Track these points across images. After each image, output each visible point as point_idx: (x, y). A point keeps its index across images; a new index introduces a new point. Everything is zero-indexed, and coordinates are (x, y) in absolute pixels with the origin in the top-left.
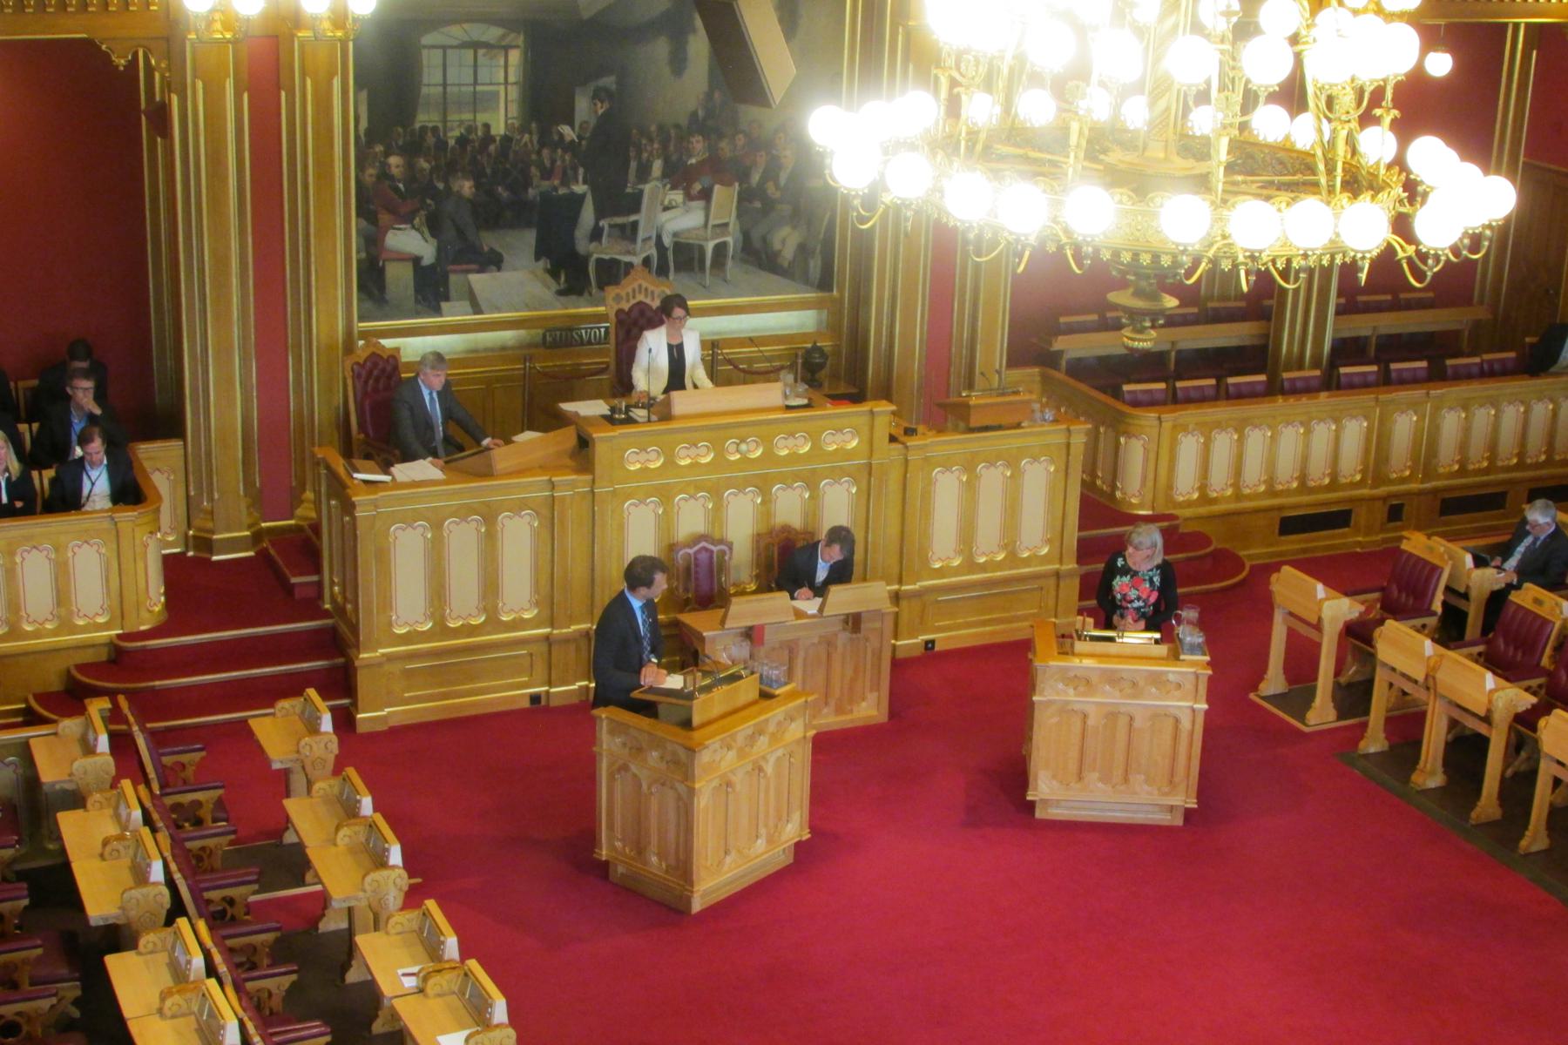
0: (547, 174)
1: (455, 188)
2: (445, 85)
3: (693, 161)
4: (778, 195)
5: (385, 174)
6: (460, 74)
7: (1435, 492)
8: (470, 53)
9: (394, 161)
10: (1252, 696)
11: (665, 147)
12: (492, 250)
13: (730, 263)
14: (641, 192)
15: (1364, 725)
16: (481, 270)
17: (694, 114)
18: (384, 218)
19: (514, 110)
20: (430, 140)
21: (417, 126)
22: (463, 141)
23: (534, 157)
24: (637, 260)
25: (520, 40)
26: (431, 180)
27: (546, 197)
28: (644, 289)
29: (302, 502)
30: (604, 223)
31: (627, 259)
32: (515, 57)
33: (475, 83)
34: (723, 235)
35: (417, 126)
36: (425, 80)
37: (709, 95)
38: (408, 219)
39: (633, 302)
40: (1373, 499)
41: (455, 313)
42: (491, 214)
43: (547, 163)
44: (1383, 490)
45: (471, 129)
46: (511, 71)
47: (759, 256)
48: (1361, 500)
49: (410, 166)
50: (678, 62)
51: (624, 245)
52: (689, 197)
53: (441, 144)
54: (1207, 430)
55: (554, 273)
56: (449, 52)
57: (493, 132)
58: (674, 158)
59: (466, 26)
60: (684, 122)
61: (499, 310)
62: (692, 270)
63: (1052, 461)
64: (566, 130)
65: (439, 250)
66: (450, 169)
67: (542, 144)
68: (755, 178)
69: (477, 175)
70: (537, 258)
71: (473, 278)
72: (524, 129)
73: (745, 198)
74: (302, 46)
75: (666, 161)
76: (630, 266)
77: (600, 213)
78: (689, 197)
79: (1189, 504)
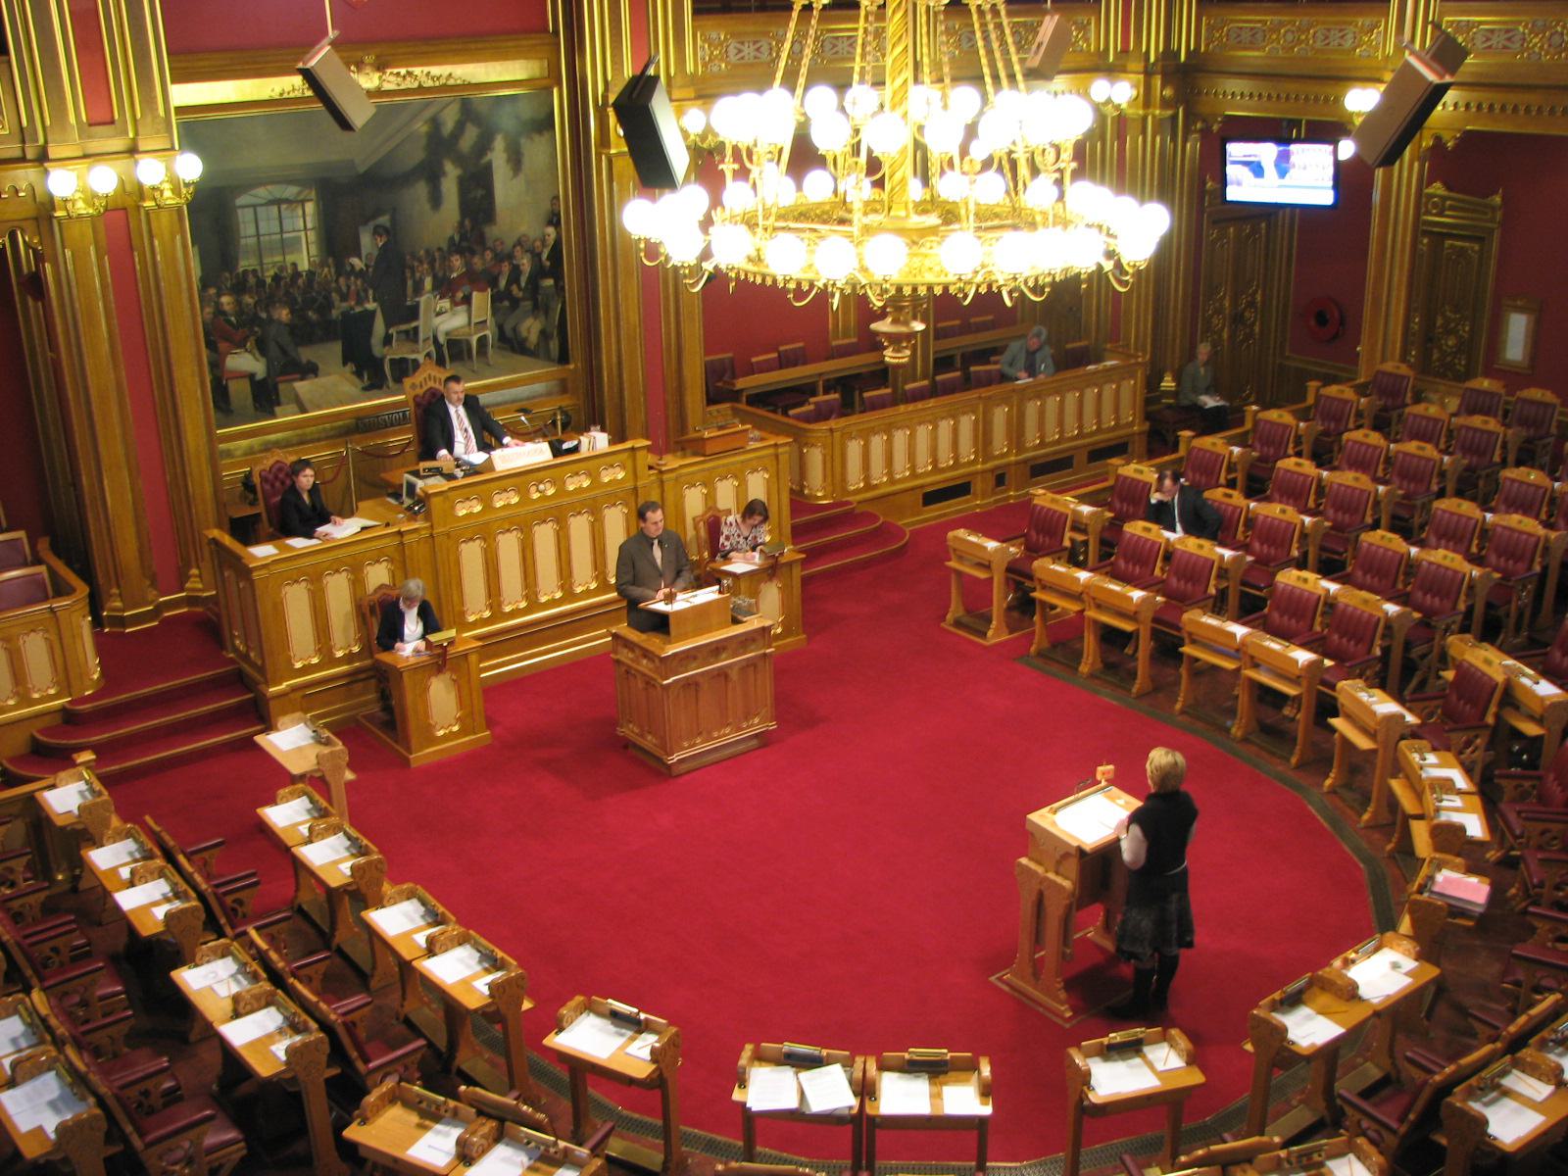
0: (344, 298)
1: (276, 316)
2: (258, 235)
3: (455, 275)
4: (521, 294)
5: (219, 311)
7: (1025, 461)
8: (275, 209)
9: (225, 299)
10: (943, 625)
11: (432, 263)
12: (309, 362)
13: (490, 350)
14: (418, 303)
15: (1034, 632)
16: (302, 379)
17: (452, 239)
18: (222, 346)
19: (314, 250)
20: (252, 280)
22: (276, 278)
23: (334, 285)
24: (420, 357)
25: (313, 195)
26: (256, 314)
27: (345, 314)
28: (428, 377)
29: (190, 577)
30: (392, 331)
31: (413, 356)
32: (310, 207)
33: (282, 232)
34: (483, 330)
36: (242, 234)
37: (461, 224)
38: (241, 345)
39: (425, 388)
40: (984, 472)
41: (286, 416)
42: (305, 333)
43: (344, 289)
44: (989, 465)
45: (282, 268)
46: (308, 219)
47: (511, 343)
48: (976, 473)
49: (239, 303)
50: (436, 200)
51: (409, 346)
52: (455, 304)
53: (261, 283)
54: (865, 435)
55: (359, 374)
56: (259, 209)
57: (300, 269)
58: (440, 274)
59: (269, 187)
60: (445, 246)
61: (320, 408)
62: (462, 359)
63: (765, 469)
64: (355, 261)
66: (269, 302)
67: (339, 274)
68: (503, 283)
69: (291, 303)
70: (345, 364)
72: (323, 264)
73: (496, 299)
74: (147, 213)
75: (435, 277)
76: (415, 361)
77: (388, 325)
78: (455, 304)
79: (858, 491)
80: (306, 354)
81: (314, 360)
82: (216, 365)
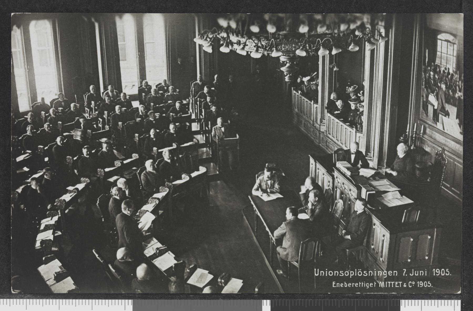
6: (444, 50)
8: (446, 43)
9: (432, 73)
16: (445, 116)
19: (454, 66)
21: (436, 64)
23: (458, 83)
35: (436, 64)
49: (434, 76)
53: (440, 71)
65: (438, 104)
70: (457, 119)
71: (443, 117)
72: (456, 73)
80: (448, 107)
81: (449, 111)
82: (427, 97)
